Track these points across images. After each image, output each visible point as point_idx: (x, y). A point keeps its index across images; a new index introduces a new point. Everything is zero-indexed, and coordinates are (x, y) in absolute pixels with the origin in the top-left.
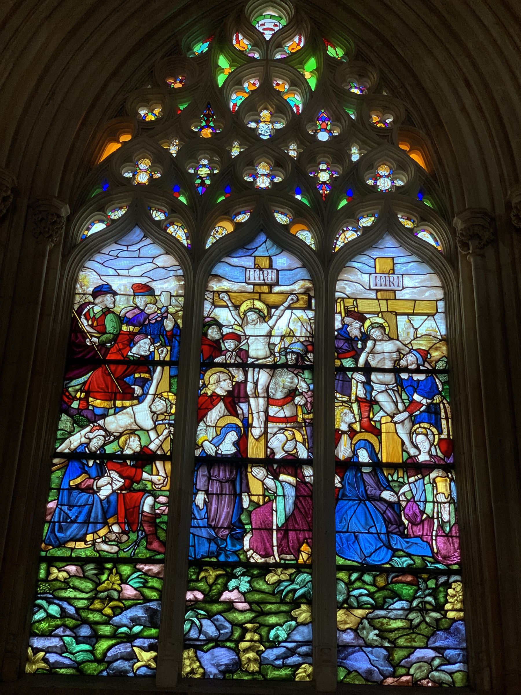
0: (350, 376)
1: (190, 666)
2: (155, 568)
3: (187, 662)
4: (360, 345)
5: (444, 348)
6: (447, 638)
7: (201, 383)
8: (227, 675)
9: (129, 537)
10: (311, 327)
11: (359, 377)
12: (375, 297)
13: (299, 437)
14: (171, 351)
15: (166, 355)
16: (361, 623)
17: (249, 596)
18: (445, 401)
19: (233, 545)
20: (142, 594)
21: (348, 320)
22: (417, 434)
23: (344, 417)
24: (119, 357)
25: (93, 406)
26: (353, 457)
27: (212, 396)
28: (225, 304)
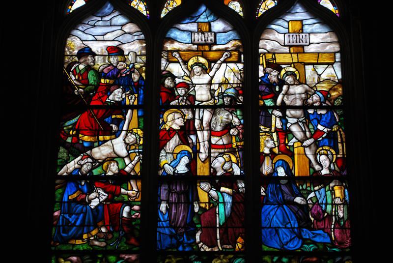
0: (270, 112)
4: (277, 89)
5: (340, 89)
7: (161, 121)
9: (113, 236)
10: (241, 76)
12: (288, 52)
13: (234, 159)
14: (138, 98)
15: (135, 100)
18: (341, 130)
19: (188, 239)
21: (268, 70)
22: (321, 155)
23: (266, 144)
24: (100, 103)
25: (83, 141)
28: (177, 60)
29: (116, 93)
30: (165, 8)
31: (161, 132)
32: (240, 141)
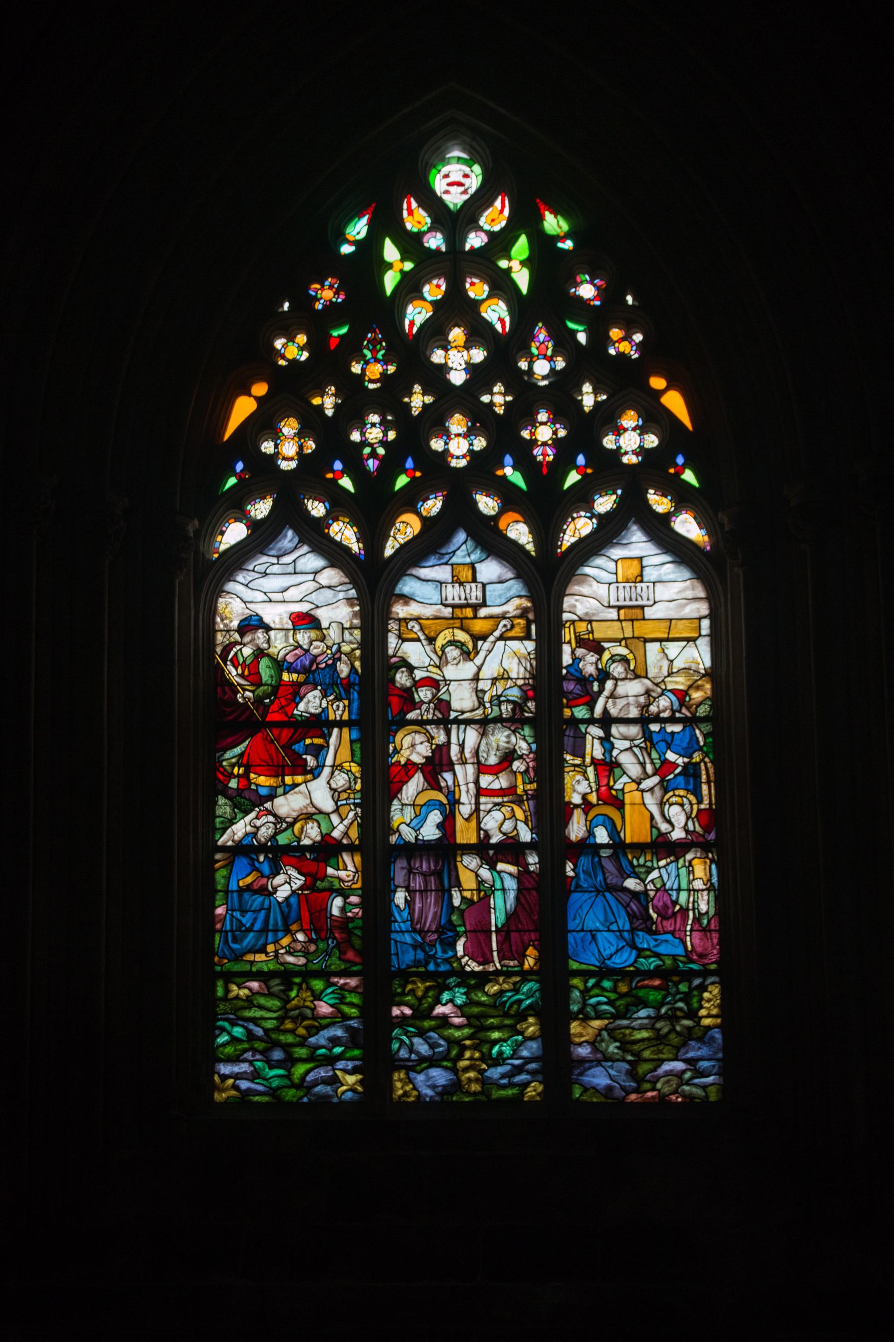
0: (583, 730)
1: (402, 1088)
2: (353, 982)
3: (399, 1085)
5: (708, 686)
6: (700, 1048)
7: (391, 748)
8: (445, 1097)
10: (531, 665)
11: (596, 731)
12: (616, 618)
13: (519, 814)
14: (349, 706)
16: (599, 1035)
17: (466, 1009)
18: (707, 760)
19: (444, 952)
20: (340, 1011)
21: (580, 652)
22: (671, 805)
25: (257, 785)
26: (589, 837)
27: (406, 764)
28: (415, 636)
29: (311, 699)
30: (391, 538)
31: (392, 768)
32: (531, 783)
